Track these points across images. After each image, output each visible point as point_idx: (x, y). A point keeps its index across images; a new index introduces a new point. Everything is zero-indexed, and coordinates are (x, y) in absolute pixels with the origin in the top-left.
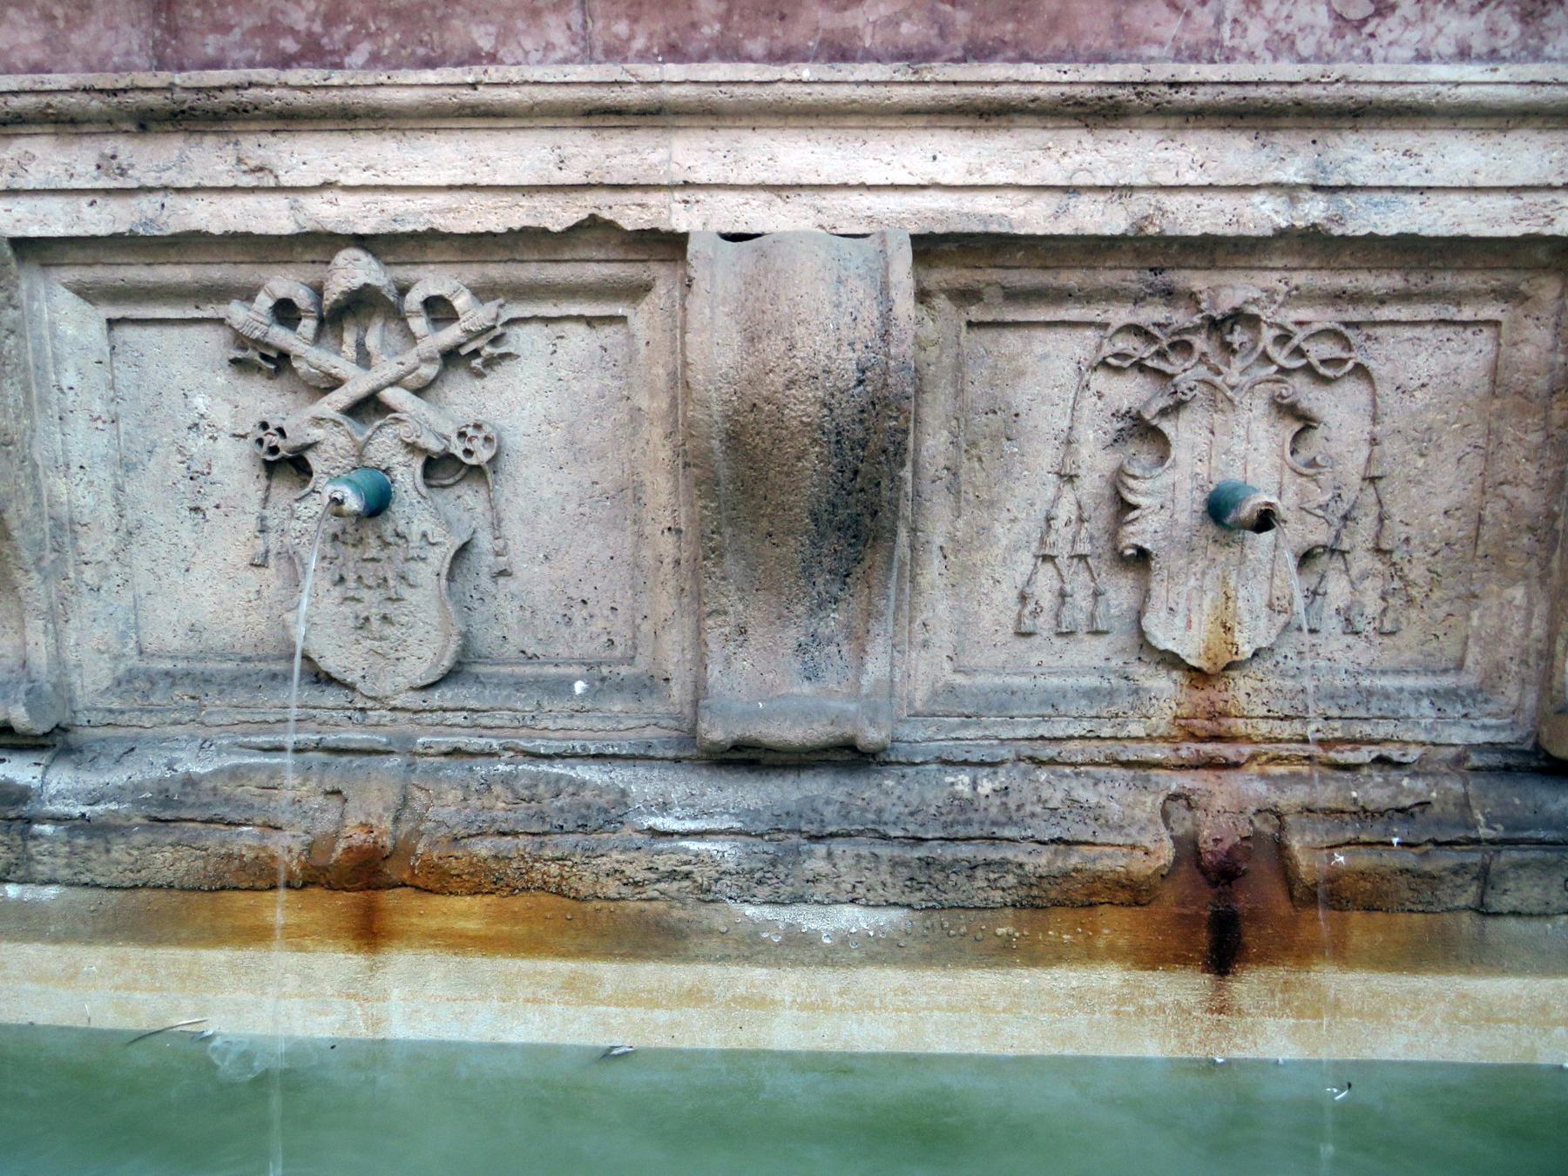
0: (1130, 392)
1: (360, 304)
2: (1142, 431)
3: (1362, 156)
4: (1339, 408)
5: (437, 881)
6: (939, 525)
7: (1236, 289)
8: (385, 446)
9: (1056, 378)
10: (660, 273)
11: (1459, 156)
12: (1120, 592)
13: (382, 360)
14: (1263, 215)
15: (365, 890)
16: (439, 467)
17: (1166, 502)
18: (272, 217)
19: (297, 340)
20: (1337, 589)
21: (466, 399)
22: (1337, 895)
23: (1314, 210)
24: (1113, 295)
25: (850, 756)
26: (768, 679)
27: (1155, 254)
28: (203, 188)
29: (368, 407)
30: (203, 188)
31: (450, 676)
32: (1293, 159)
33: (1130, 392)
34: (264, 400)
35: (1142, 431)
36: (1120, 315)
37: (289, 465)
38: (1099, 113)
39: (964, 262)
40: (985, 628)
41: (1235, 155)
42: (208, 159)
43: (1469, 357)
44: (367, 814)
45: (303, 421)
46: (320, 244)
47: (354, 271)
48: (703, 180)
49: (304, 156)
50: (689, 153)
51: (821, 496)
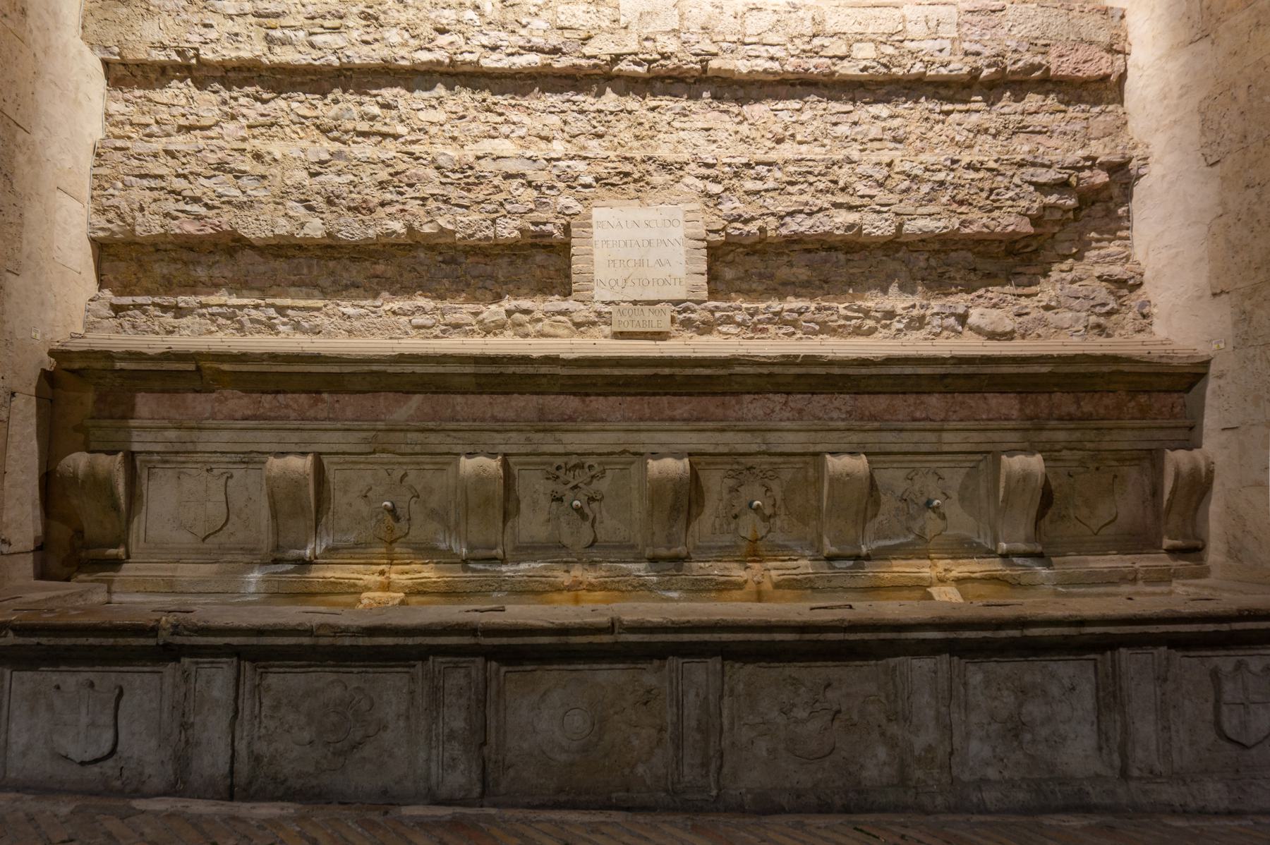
0: (731, 482)
1: (575, 467)
3: (772, 437)
4: (775, 486)
11: (790, 437)
13: (581, 477)
18: (561, 449)
20: (778, 523)
21: (596, 484)
23: (764, 448)
24: (727, 463)
28: (548, 444)
30: (548, 444)
31: (591, 546)
33: (731, 482)
34: (551, 485)
35: (733, 490)
36: (729, 467)
38: (723, 430)
42: (549, 437)
47: (574, 460)
49: (567, 437)
50: (644, 437)
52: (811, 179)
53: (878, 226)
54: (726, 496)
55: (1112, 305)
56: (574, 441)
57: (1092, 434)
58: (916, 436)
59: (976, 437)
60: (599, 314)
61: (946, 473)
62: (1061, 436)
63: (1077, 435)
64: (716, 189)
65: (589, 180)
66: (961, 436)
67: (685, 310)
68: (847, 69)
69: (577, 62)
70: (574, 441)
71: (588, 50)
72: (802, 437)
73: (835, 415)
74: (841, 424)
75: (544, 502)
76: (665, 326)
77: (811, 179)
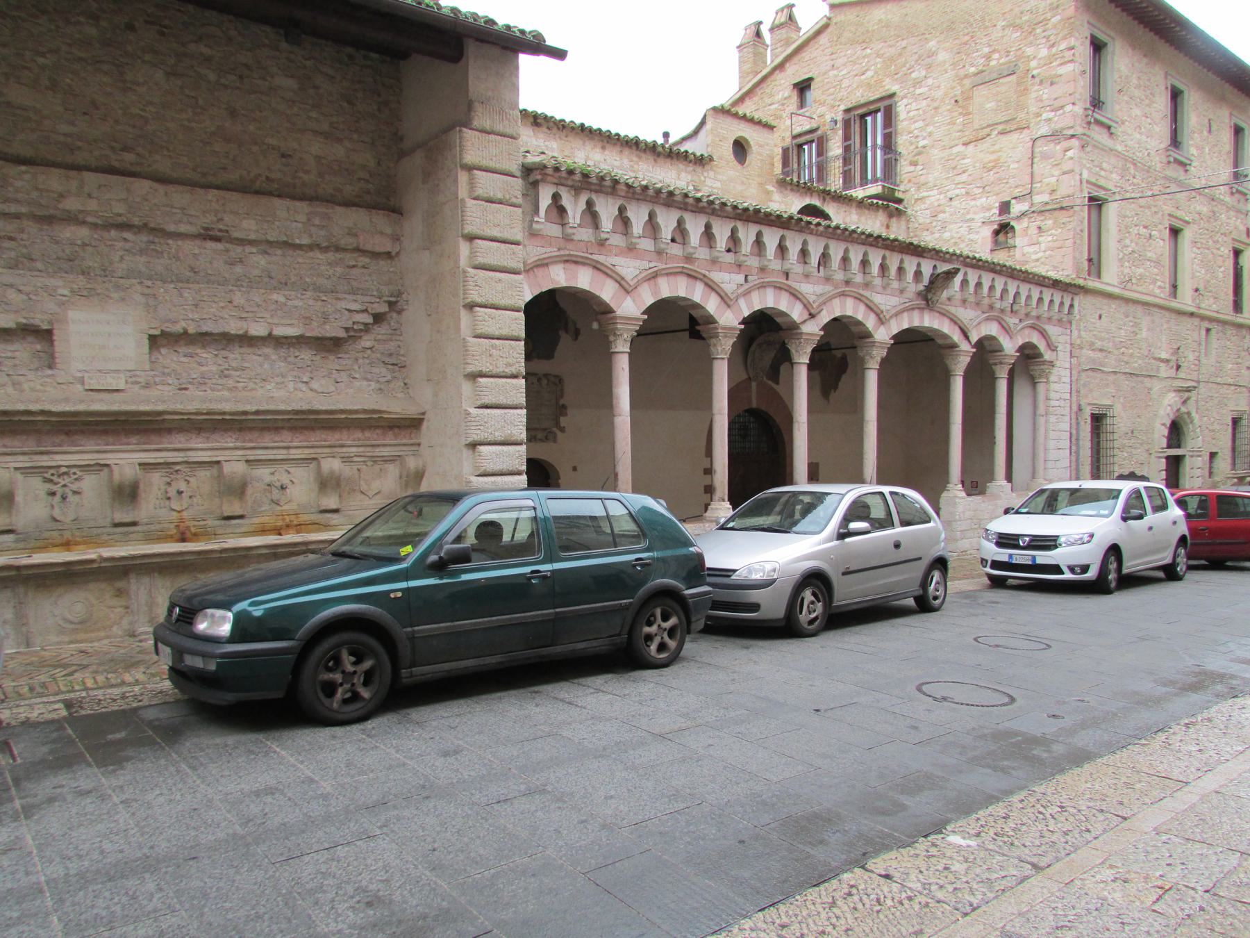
1: (64, 473)
2: (169, 484)
5: (77, 544)
6: (143, 495)
7: (178, 467)
8: (67, 490)
9: (157, 478)
10: (106, 469)
12: (167, 502)
13: (67, 480)
14: (180, 460)
15: (67, 545)
16: (75, 493)
17: (172, 492)
18: (54, 464)
19: (55, 478)
22: (195, 535)
25: (134, 524)
26: (120, 517)
27: (168, 464)
28: (45, 461)
29: (65, 486)
30: (45, 461)
32: (182, 454)
34: (48, 486)
35: (169, 484)
37: (53, 494)
39: (144, 466)
40: (150, 508)
41: (176, 454)
42: (45, 457)
43: (208, 473)
44: (67, 535)
45: (54, 488)
46: (59, 467)
47: (64, 470)
48: (109, 458)
49: (58, 457)
51: (128, 493)
52: (216, 299)
53: (258, 330)
54: (163, 488)
55: (389, 377)
56: (61, 460)
57: (368, 449)
58: (275, 452)
59: (307, 451)
60: (75, 378)
61: (291, 470)
62: (354, 449)
63: (361, 449)
64: (152, 302)
65: (66, 292)
66: (299, 451)
67: (135, 376)
68: (236, 234)
69: (52, 212)
70: (61, 460)
71: (60, 206)
72: (209, 453)
73: (229, 440)
74: (231, 445)
75: (42, 494)
76: (122, 386)
77: (216, 299)
